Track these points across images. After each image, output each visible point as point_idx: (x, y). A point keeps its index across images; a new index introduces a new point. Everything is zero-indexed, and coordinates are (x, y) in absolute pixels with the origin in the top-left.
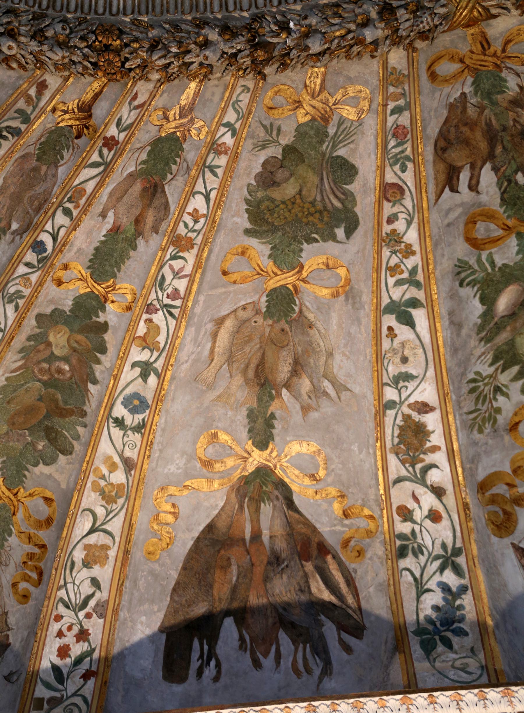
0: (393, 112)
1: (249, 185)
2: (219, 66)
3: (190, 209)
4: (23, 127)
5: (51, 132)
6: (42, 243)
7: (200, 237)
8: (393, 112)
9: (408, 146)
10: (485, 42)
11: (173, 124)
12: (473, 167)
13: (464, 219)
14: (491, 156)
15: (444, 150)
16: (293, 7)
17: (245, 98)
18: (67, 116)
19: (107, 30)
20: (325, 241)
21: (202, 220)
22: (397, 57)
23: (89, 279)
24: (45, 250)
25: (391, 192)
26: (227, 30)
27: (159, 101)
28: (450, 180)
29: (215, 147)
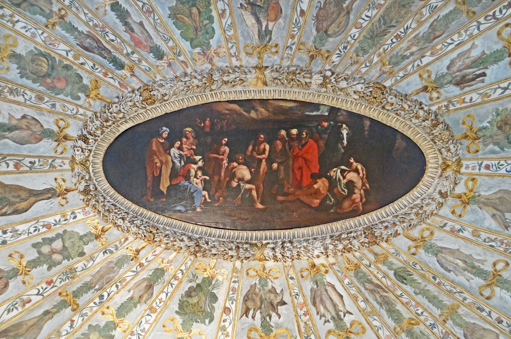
0: (233, 282)
1: (182, 294)
2: (184, 249)
3: (159, 297)
4: (115, 251)
5: (123, 256)
6: (103, 296)
7: (160, 309)
8: (233, 282)
9: (235, 295)
10: (264, 269)
11: (164, 265)
12: (254, 310)
13: (248, 328)
14: (260, 308)
15: (246, 301)
16: (212, 238)
17: (189, 263)
18: (131, 252)
19: (153, 227)
20: (201, 323)
21: (162, 303)
22: (238, 264)
23: (115, 315)
24: (103, 299)
25: (227, 310)
26: (190, 238)
27: (162, 256)
28: (246, 312)
29: (175, 277)
